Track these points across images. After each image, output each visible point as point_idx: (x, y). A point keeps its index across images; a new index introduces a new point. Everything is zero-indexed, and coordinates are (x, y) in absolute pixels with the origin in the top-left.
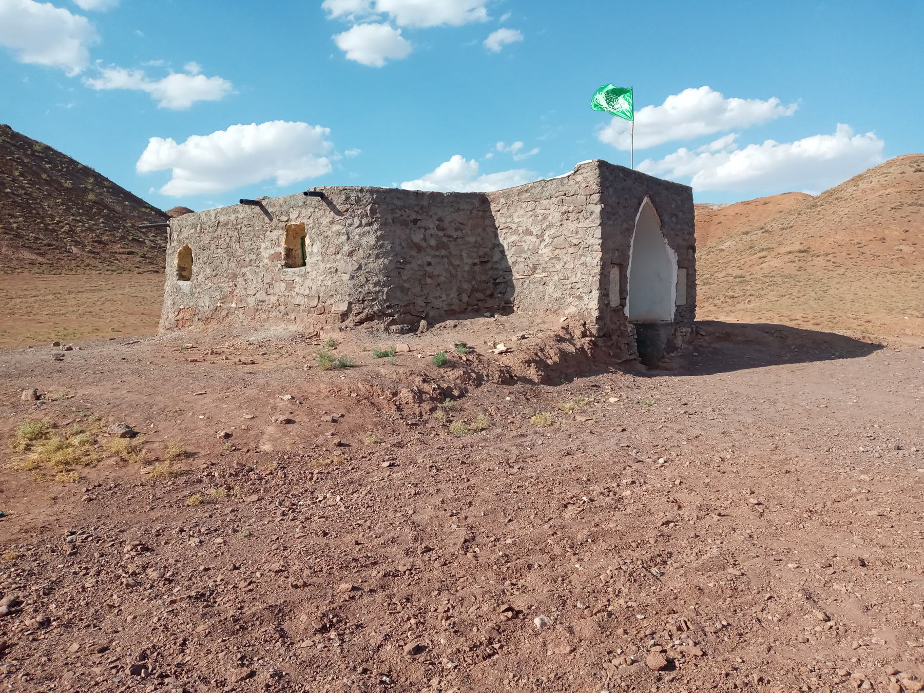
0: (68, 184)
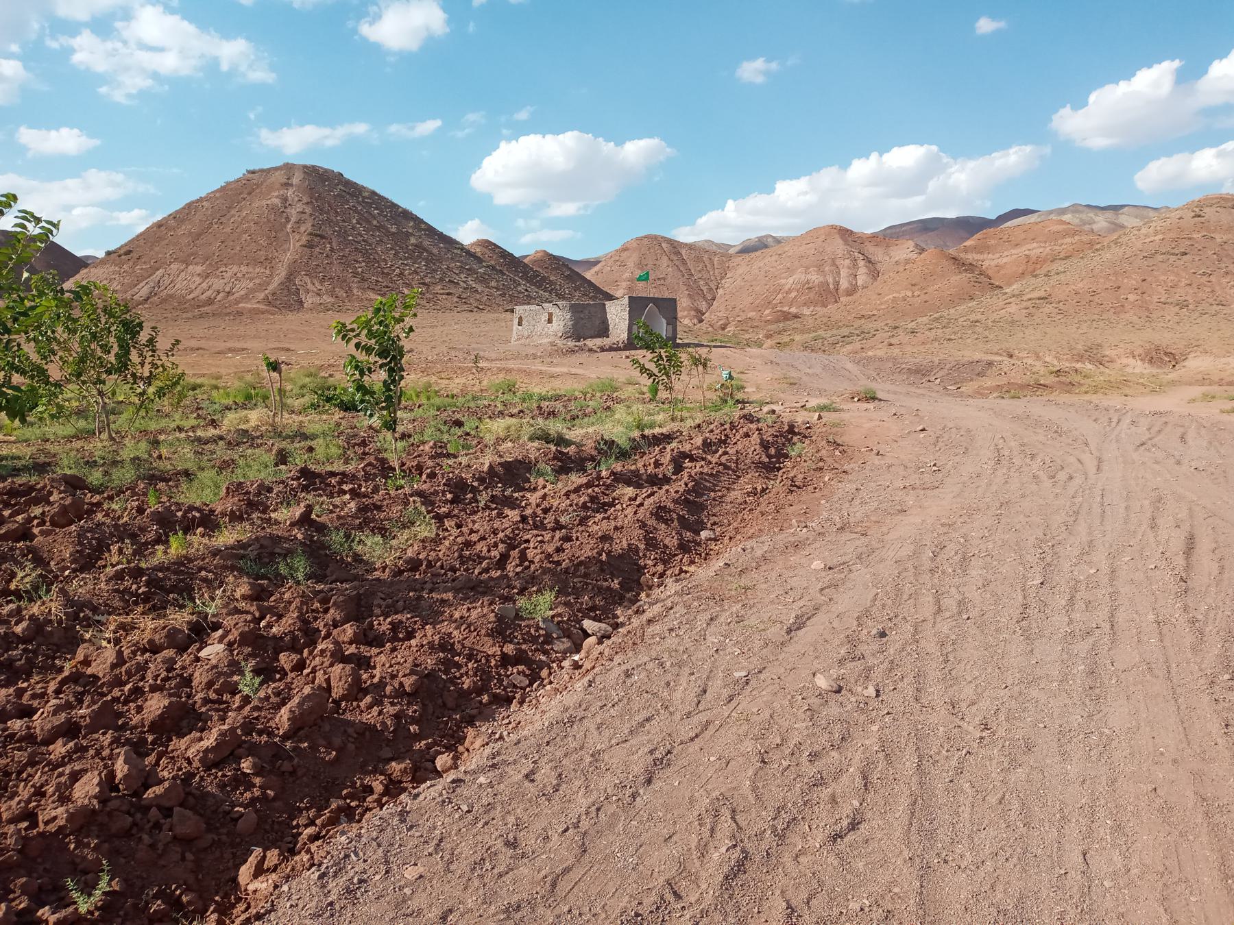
0: (394, 229)
